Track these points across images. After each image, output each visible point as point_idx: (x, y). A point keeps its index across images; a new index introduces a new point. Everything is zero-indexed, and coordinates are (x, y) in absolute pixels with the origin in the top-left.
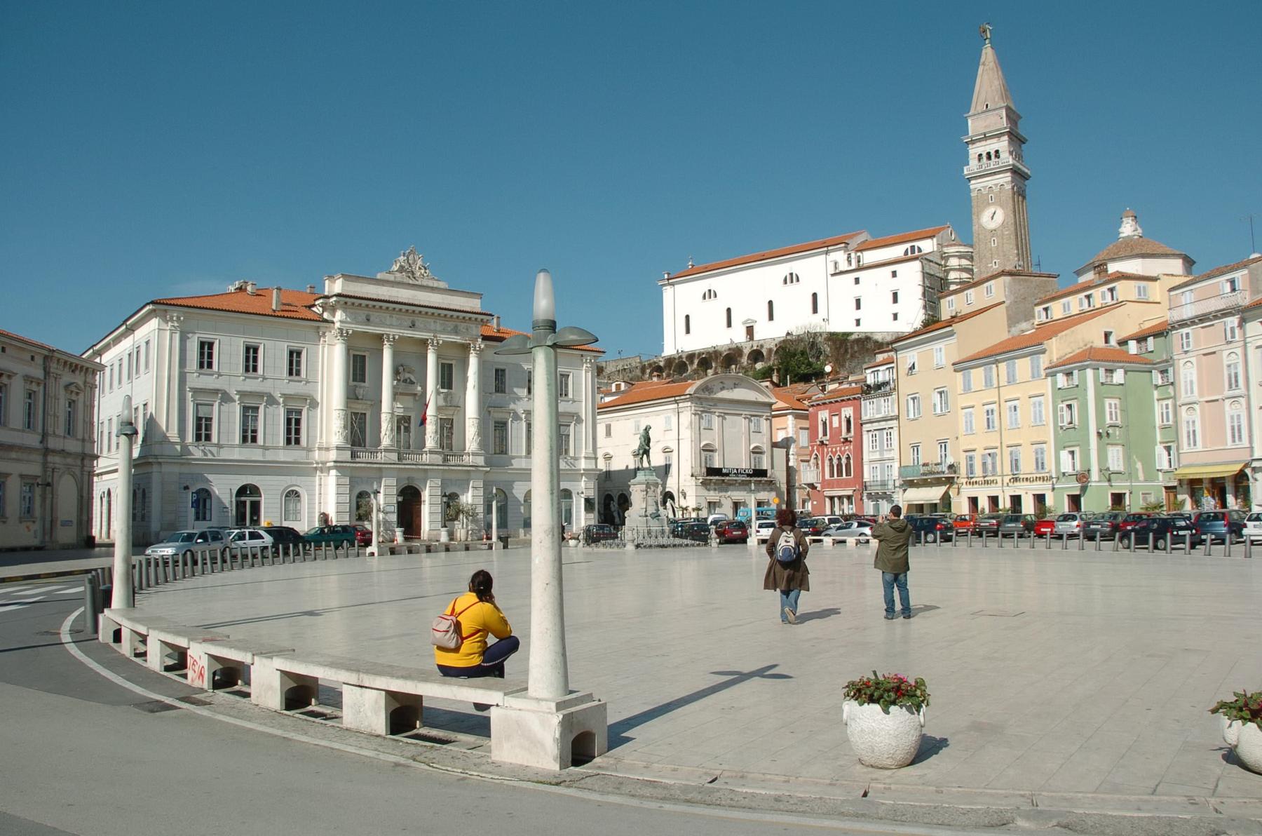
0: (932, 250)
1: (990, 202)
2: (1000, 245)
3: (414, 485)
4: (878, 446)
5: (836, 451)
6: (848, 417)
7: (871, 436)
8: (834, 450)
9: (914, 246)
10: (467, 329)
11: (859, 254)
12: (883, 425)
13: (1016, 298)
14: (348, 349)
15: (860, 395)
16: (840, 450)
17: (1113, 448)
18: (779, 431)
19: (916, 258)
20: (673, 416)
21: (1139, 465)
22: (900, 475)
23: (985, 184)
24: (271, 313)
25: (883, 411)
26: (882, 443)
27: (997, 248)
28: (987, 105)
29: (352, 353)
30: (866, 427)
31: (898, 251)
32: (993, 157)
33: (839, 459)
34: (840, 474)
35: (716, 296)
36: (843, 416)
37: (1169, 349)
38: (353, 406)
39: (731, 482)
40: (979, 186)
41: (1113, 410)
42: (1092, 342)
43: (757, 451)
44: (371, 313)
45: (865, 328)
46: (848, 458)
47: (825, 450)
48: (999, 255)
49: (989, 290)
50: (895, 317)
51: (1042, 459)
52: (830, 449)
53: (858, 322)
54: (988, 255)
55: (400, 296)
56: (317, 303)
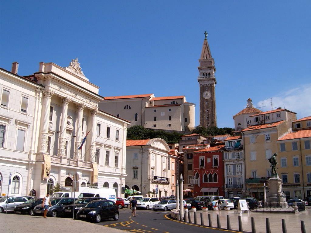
5: (209, 172)
8: (208, 171)
13: (289, 119)
20: (139, 153)
23: (205, 83)
27: (208, 105)
30: (225, 164)
32: (208, 74)
33: (210, 176)
34: (211, 181)
36: (213, 159)
40: (203, 84)
45: (157, 128)
46: (215, 176)
47: (203, 171)
52: (205, 171)
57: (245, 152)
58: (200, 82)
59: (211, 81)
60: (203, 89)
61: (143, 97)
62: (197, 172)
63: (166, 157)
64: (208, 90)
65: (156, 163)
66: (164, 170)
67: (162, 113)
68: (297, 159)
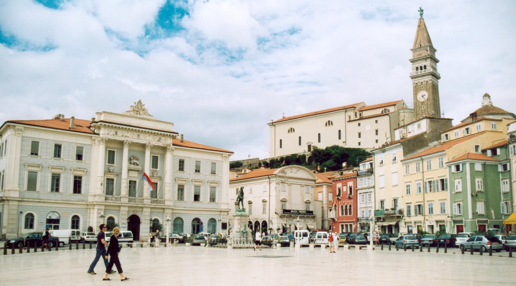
0: (394, 111)
1: (422, 89)
2: (426, 109)
3: (136, 214)
4: (365, 200)
5: (345, 203)
6: (351, 186)
7: (361, 196)
8: (344, 202)
9: (386, 109)
10: (165, 140)
11: (361, 112)
12: (367, 190)
14: (106, 148)
15: (356, 176)
16: (347, 202)
17: (479, 203)
18: (319, 193)
19: (387, 114)
21: (492, 212)
22: (375, 215)
23: (418, 81)
24: (68, 129)
25: (367, 184)
26: (366, 199)
27: (425, 110)
28: (421, 45)
29: (108, 149)
30: (359, 192)
31: (379, 111)
33: (346, 206)
34: (346, 214)
35: (294, 131)
37: (507, 154)
38: (108, 175)
39: (294, 217)
40: (416, 82)
41: (480, 184)
42: (469, 151)
43: (308, 203)
44: (118, 131)
46: (350, 206)
47: (340, 202)
48: (425, 113)
49: (419, 126)
50: (377, 141)
51: (444, 207)
52: (342, 202)
53: (359, 144)
54: (421, 113)
55: (132, 123)
56: (92, 125)
57: (375, 176)
58: (414, 80)
59: (427, 77)
60: (417, 89)
61: (346, 109)
62: (335, 203)
63: (310, 187)
64: (423, 90)
65: (290, 194)
66: (308, 202)
67: (367, 126)
68: (420, 184)
